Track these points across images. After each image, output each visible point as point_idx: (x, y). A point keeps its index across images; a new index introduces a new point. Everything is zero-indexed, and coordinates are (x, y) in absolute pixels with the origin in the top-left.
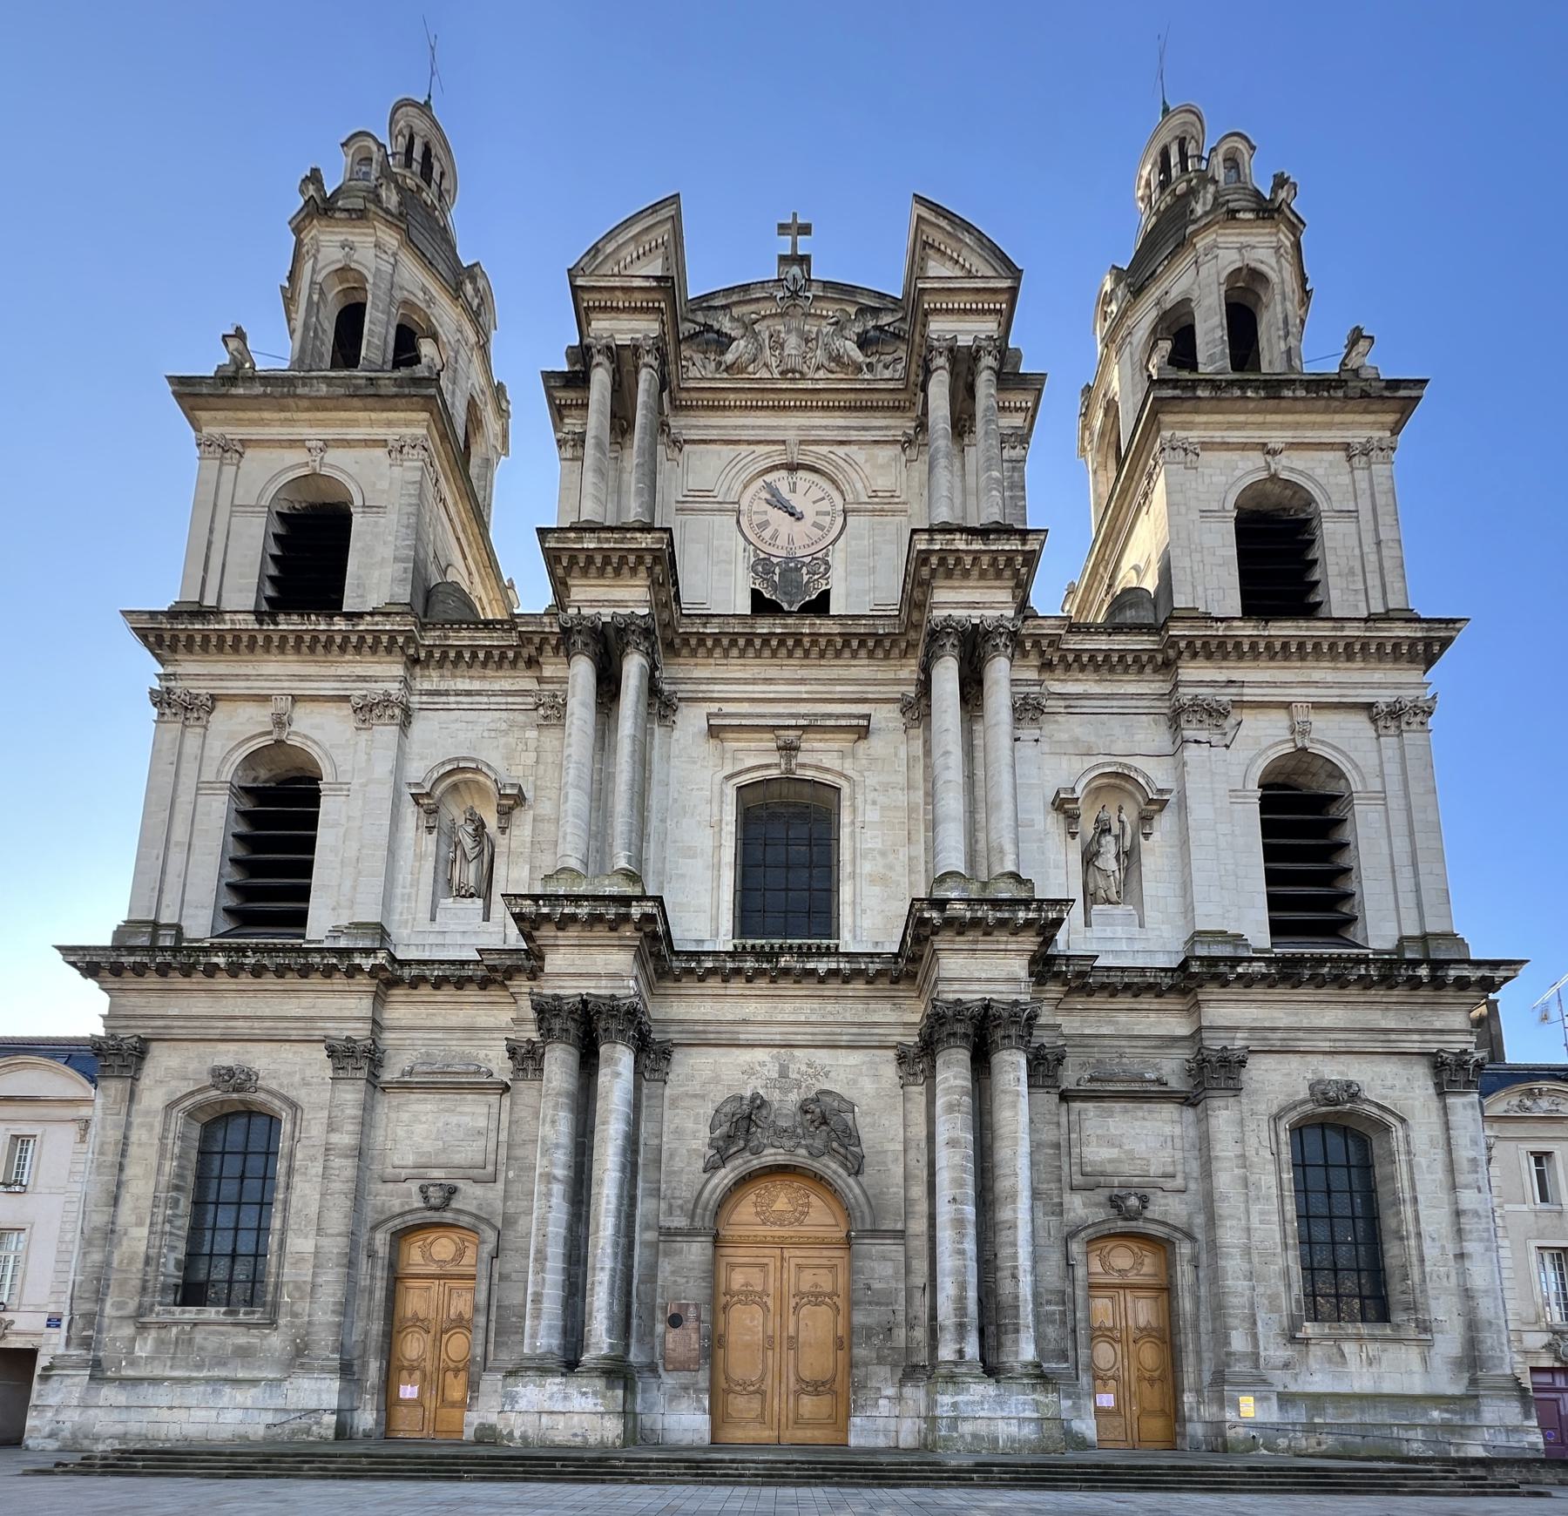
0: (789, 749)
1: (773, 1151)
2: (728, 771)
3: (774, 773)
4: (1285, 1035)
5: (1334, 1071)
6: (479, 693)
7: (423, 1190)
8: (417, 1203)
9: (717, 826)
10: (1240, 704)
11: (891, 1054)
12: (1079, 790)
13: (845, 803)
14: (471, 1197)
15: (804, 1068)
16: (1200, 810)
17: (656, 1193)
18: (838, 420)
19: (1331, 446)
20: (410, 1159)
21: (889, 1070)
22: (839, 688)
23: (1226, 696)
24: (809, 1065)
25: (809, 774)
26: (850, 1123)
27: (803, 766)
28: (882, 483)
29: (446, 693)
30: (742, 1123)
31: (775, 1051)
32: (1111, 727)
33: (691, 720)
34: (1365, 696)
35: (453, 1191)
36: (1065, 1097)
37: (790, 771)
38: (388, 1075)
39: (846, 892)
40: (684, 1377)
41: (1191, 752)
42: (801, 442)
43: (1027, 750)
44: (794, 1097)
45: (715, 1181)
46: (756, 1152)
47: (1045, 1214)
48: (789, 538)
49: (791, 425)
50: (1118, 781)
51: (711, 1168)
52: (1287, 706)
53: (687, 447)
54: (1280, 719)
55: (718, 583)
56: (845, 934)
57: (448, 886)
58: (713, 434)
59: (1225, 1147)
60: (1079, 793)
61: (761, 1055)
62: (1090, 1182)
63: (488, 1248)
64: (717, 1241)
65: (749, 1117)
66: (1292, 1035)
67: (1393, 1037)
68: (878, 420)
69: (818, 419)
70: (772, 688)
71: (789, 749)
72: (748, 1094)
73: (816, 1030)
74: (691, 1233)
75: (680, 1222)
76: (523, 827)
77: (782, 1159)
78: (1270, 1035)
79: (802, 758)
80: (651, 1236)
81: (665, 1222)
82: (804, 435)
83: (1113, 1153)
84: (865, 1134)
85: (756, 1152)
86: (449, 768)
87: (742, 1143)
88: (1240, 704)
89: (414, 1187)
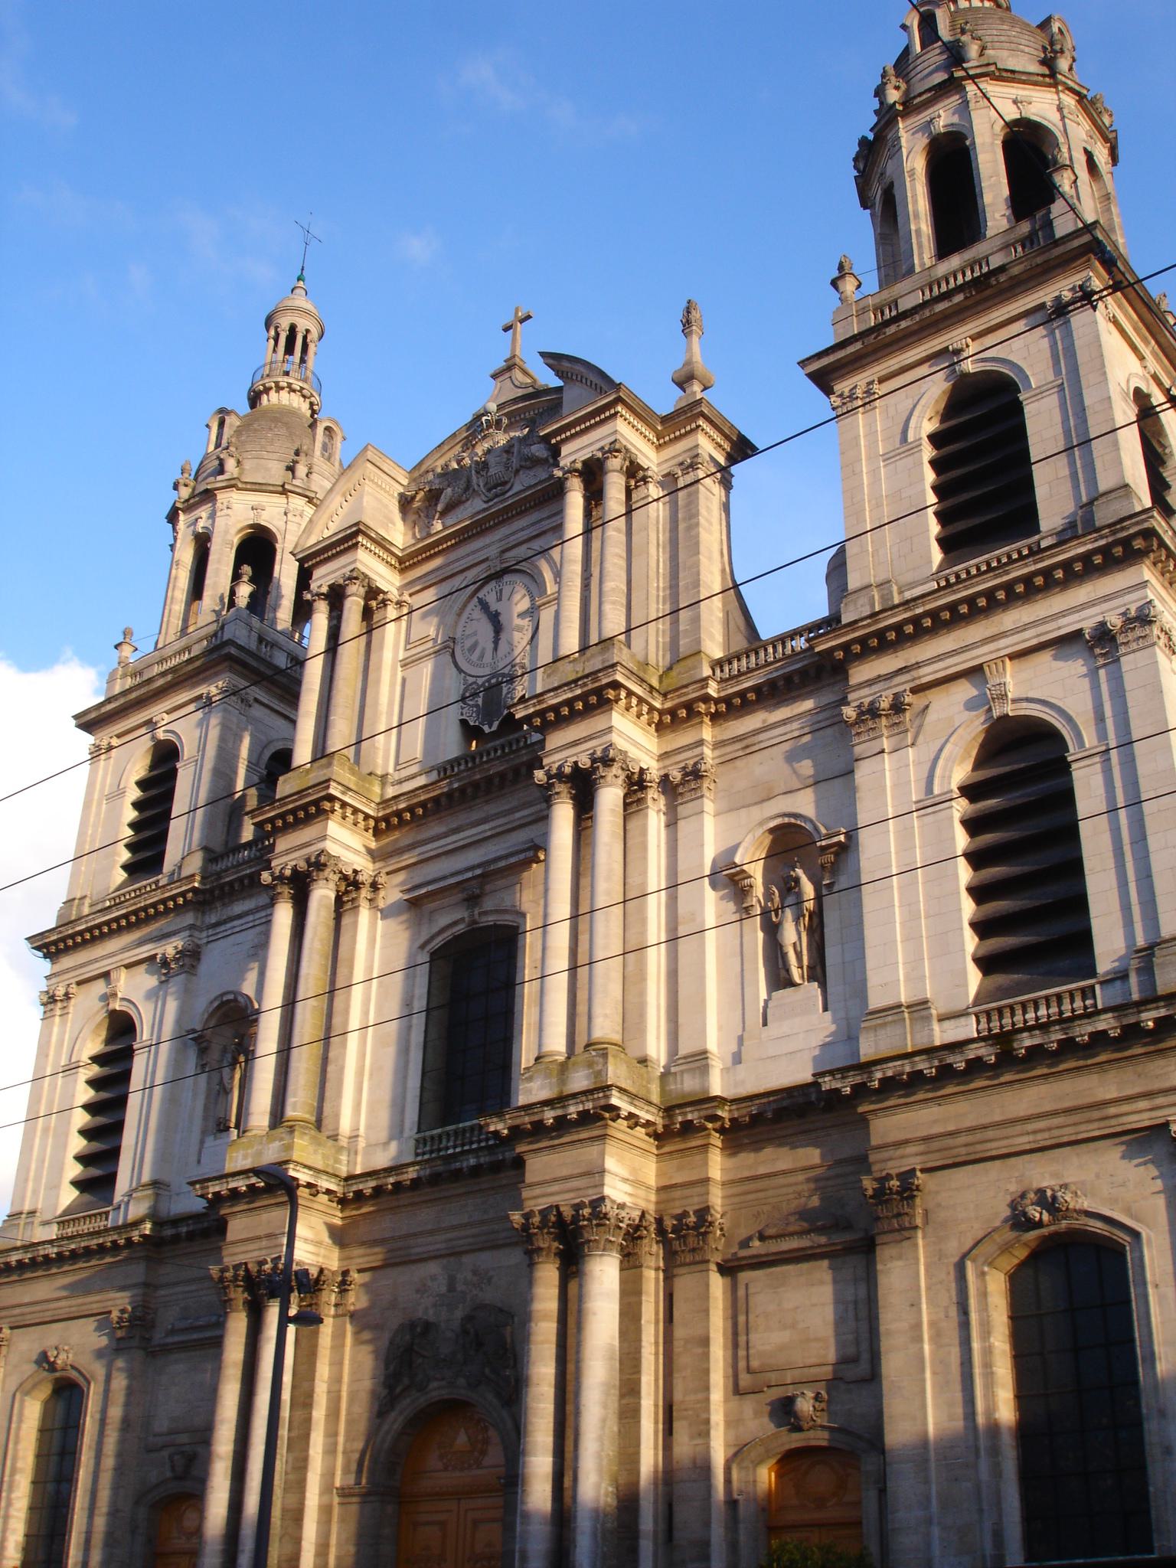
0: (472, 900)
1: (435, 1384)
3: (460, 928)
4: (970, 1138)
5: (1041, 1174)
8: (169, 1474)
15: (469, 1276)
18: (534, 516)
22: (518, 815)
24: (475, 1272)
25: (490, 920)
26: (509, 1340)
27: (486, 913)
29: (225, 922)
31: (445, 1261)
34: (1067, 625)
37: (475, 922)
38: (158, 1337)
42: (503, 552)
44: (459, 1314)
45: (385, 1427)
47: (692, 1438)
54: (965, 690)
61: (433, 1268)
66: (979, 1136)
67: (1112, 1111)
70: (462, 835)
71: (472, 900)
73: (474, 1231)
78: (950, 1142)
79: (488, 904)
82: (504, 545)
86: (216, 1004)
87: (406, 1381)
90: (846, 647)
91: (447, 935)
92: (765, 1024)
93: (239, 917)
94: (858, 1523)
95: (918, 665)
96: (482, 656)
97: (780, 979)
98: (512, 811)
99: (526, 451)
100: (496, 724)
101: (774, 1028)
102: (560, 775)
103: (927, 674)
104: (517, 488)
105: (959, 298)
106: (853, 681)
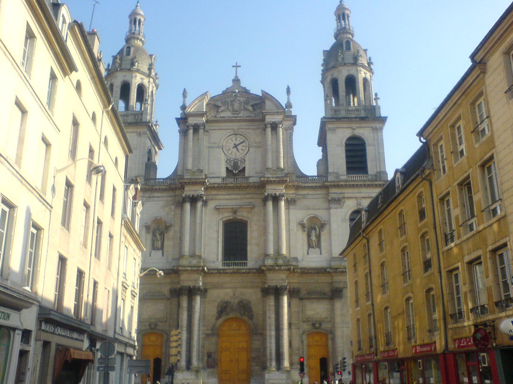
0: (235, 212)
2: (220, 217)
3: (231, 218)
6: (160, 197)
7: (150, 325)
8: (148, 328)
9: (218, 232)
10: (344, 198)
11: (259, 290)
12: (304, 221)
13: (249, 225)
14: (161, 326)
16: (334, 226)
17: (204, 326)
18: (247, 123)
19: (368, 127)
20: (146, 317)
21: (259, 294)
23: (341, 196)
25: (240, 218)
28: (258, 139)
29: (152, 197)
30: (223, 309)
32: (312, 205)
33: (212, 205)
35: (156, 325)
36: (301, 299)
39: (249, 248)
40: (211, 370)
41: (332, 211)
43: (292, 211)
44: (237, 301)
46: (228, 314)
48: (236, 155)
49: (235, 125)
50: (314, 219)
51: (217, 319)
52: (356, 198)
53: (210, 131)
55: (218, 169)
56: (249, 258)
57: (154, 248)
58: (216, 128)
59: (338, 312)
60: (305, 221)
61: (229, 290)
62: (307, 320)
63: (165, 338)
64: (218, 335)
65: (226, 307)
68: (257, 123)
69: (242, 124)
71: (235, 212)
72: (226, 300)
74: (213, 335)
75: (210, 332)
76: (171, 233)
77: (234, 316)
79: (238, 214)
80: (203, 336)
81: (206, 332)
83: (312, 313)
84: (254, 309)
85: (228, 314)
88: (344, 198)
89: (147, 324)
90: (331, 185)
91: (228, 218)
92: (308, 254)
93: (158, 197)
94: (327, 345)
95: (344, 193)
96: (232, 153)
97: (310, 246)
98: (245, 194)
99: (246, 107)
100: (237, 172)
101: (310, 256)
102: (271, 195)
103: (346, 195)
104: (241, 115)
105: (358, 119)
106: (330, 191)
